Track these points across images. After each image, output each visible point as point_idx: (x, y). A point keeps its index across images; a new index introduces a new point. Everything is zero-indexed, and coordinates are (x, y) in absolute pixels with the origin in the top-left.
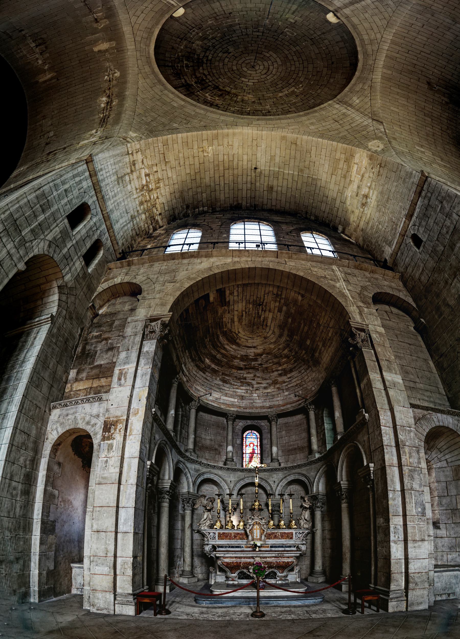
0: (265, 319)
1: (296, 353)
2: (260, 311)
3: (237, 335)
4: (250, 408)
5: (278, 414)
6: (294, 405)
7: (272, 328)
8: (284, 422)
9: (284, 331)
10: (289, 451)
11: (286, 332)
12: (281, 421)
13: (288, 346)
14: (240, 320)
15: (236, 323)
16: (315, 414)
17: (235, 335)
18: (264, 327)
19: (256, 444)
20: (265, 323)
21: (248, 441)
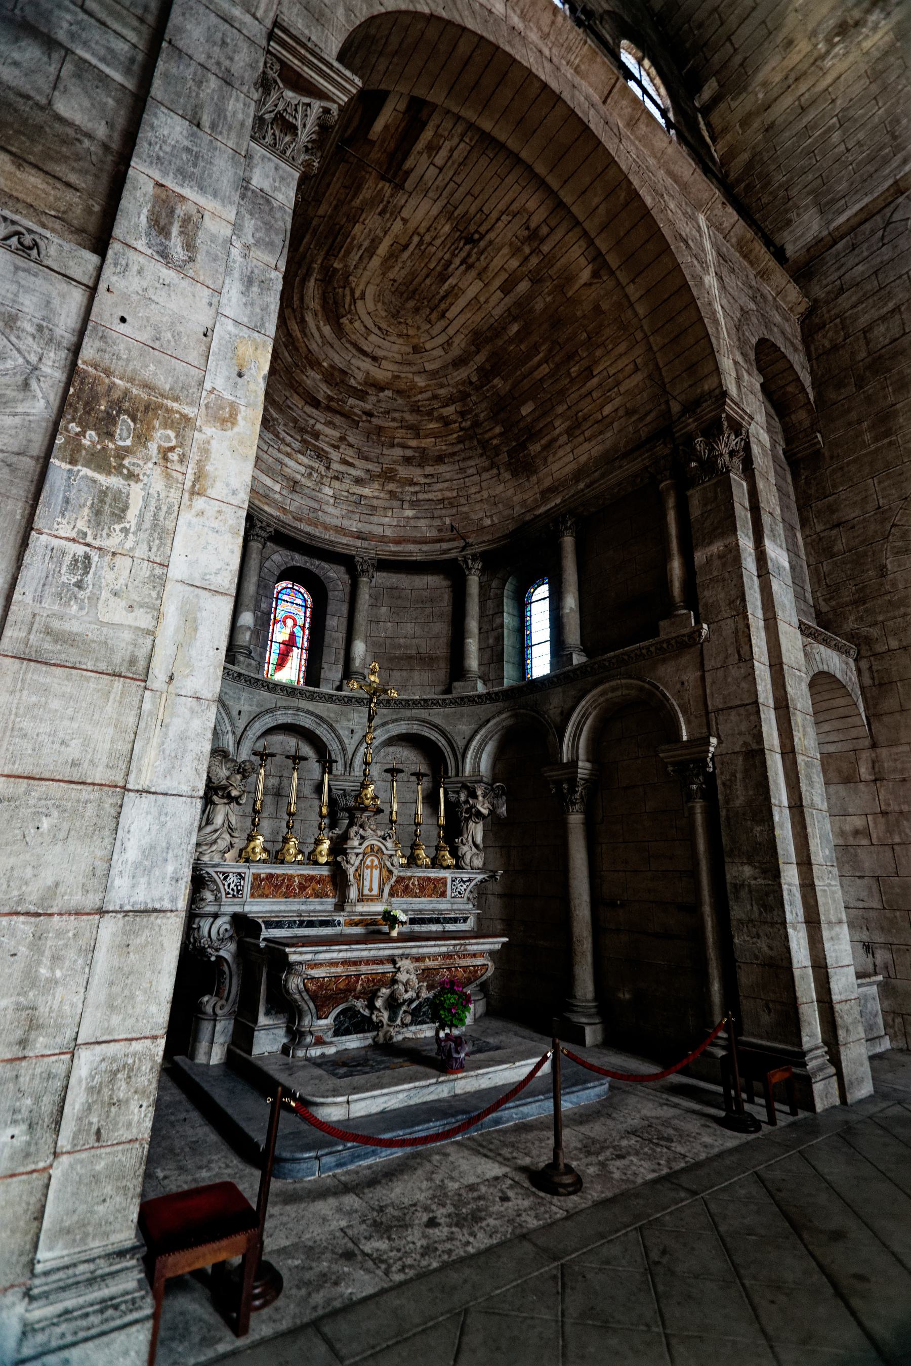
0: (454, 293)
1: (476, 424)
2: (457, 261)
3: (354, 301)
4: (310, 523)
5: (380, 560)
6: (425, 548)
7: (451, 331)
8: (388, 584)
9: (478, 352)
10: (392, 659)
11: (480, 358)
12: (381, 578)
13: (463, 396)
14: (392, 257)
15: (376, 262)
16: (481, 587)
17: (348, 298)
18: (434, 316)
19: (300, 622)
20: (443, 306)
21: (282, 610)
